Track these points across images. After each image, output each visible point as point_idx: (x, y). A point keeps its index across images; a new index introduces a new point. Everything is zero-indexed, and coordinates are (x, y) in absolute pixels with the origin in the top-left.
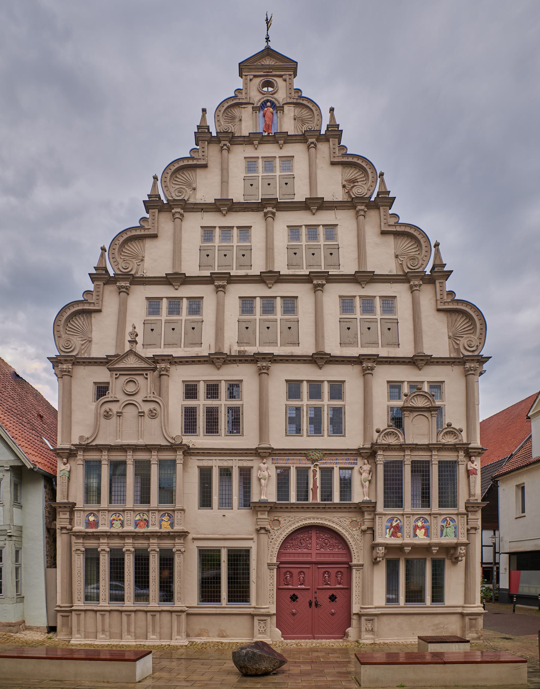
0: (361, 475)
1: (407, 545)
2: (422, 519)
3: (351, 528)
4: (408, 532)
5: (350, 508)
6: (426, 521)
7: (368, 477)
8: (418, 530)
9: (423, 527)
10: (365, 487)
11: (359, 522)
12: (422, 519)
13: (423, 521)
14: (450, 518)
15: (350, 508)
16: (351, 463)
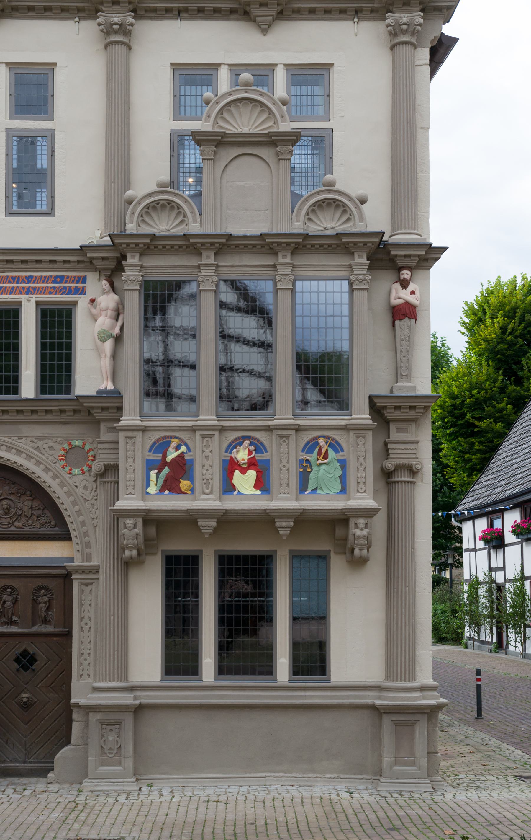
0: (96, 321)
1: (206, 514)
2: (247, 442)
3: (67, 469)
4: (208, 477)
5: (62, 411)
6: (259, 447)
7: (113, 327)
8: (237, 473)
9: (252, 464)
10: (103, 355)
11: (89, 451)
12: (247, 442)
13: (252, 448)
14: (329, 438)
15: (62, 411)
16: (69, 291)
